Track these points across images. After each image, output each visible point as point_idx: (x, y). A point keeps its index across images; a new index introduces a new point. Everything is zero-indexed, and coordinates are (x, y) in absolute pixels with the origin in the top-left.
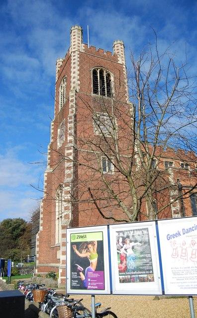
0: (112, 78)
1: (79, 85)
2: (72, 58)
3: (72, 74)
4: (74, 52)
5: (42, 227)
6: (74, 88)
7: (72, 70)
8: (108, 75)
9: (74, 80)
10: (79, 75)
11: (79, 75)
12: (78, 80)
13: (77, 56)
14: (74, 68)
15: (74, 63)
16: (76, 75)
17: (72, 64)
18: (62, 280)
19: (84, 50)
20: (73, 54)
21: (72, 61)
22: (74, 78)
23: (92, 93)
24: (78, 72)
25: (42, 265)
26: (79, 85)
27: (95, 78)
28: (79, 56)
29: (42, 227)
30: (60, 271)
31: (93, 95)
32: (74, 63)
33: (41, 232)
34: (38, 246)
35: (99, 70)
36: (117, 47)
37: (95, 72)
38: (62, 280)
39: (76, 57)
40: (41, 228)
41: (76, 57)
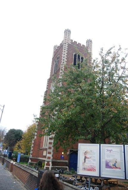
1: (66, 61)
2: (64, 46)
3: (63, 55)
4: (65, 43)
6: (63, 62)
9: (64, 58)
10: (67, 56)
11: (67, 56)
13: (67, 45)
14: (65, 52)
15: (65, 49)
16: (65, 56)
17: (64, 49)
18: (46, 167)
20: (64, 44)
21: (64, 48)
22: (64, 57)
24: (66, 55)
25: (34, 158)
26: (66, 61)
30: (46, 163)
32: (65, 49)
33: (35, 139)
34: (33, 147)
35: (78, 54)
36: (89, 43)
37: (75, 56)
38: (46, 167)
39: (66, 46)
40: (35, 137)
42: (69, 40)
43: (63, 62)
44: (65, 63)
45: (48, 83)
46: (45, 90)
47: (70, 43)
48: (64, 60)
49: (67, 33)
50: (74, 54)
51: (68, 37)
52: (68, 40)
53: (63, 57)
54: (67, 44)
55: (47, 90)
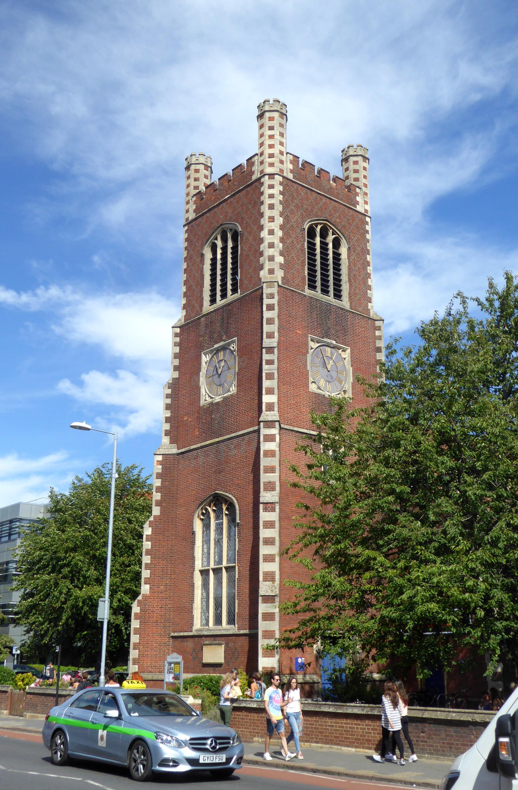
0: (343, 250)
4: (271, 176)
5: (147, 587)
7: (267, 225)
8: (337, 243)
12: (281, 254)
19: (291, 171)
23: (307, 287)
27: (312, 246)
28: (281, 188)
29: (147, 587)
31: (308, 292)
35: (319, 227)
37: (311, 233)
39: (275, 191)
40: (145, 589)
41: (275, 191)
42: (284, 158)
43: (271, 271)
44: (279, 274)
45: (176, 344)
46: (168, 375)
47: (291, 176)
48: (271, 259)
49: (275, 123)
50: (306, 227)
51: (281, 144)
52: (282, 162)
53: (266, 243)
54: (279, 178)
55: (176, 375)
